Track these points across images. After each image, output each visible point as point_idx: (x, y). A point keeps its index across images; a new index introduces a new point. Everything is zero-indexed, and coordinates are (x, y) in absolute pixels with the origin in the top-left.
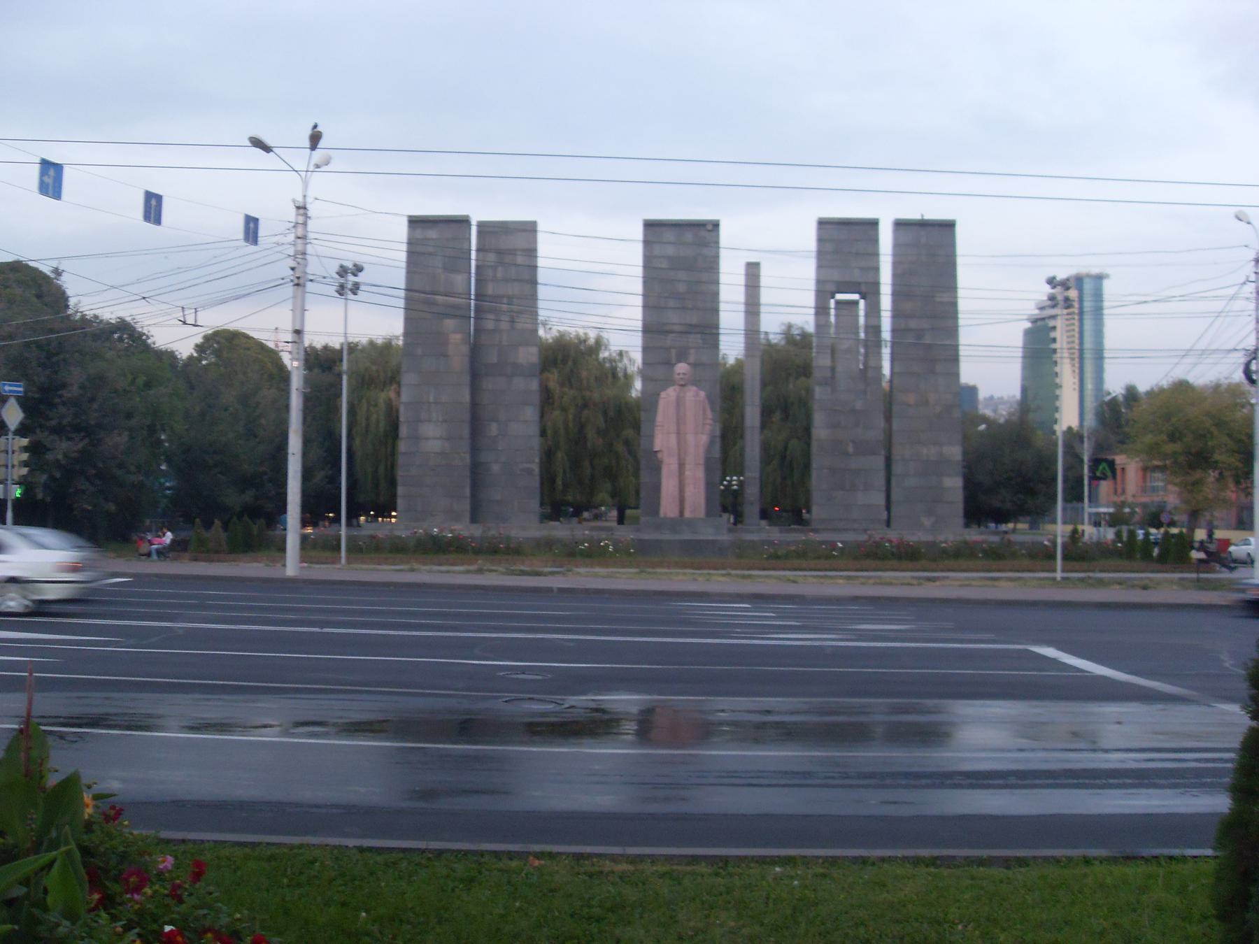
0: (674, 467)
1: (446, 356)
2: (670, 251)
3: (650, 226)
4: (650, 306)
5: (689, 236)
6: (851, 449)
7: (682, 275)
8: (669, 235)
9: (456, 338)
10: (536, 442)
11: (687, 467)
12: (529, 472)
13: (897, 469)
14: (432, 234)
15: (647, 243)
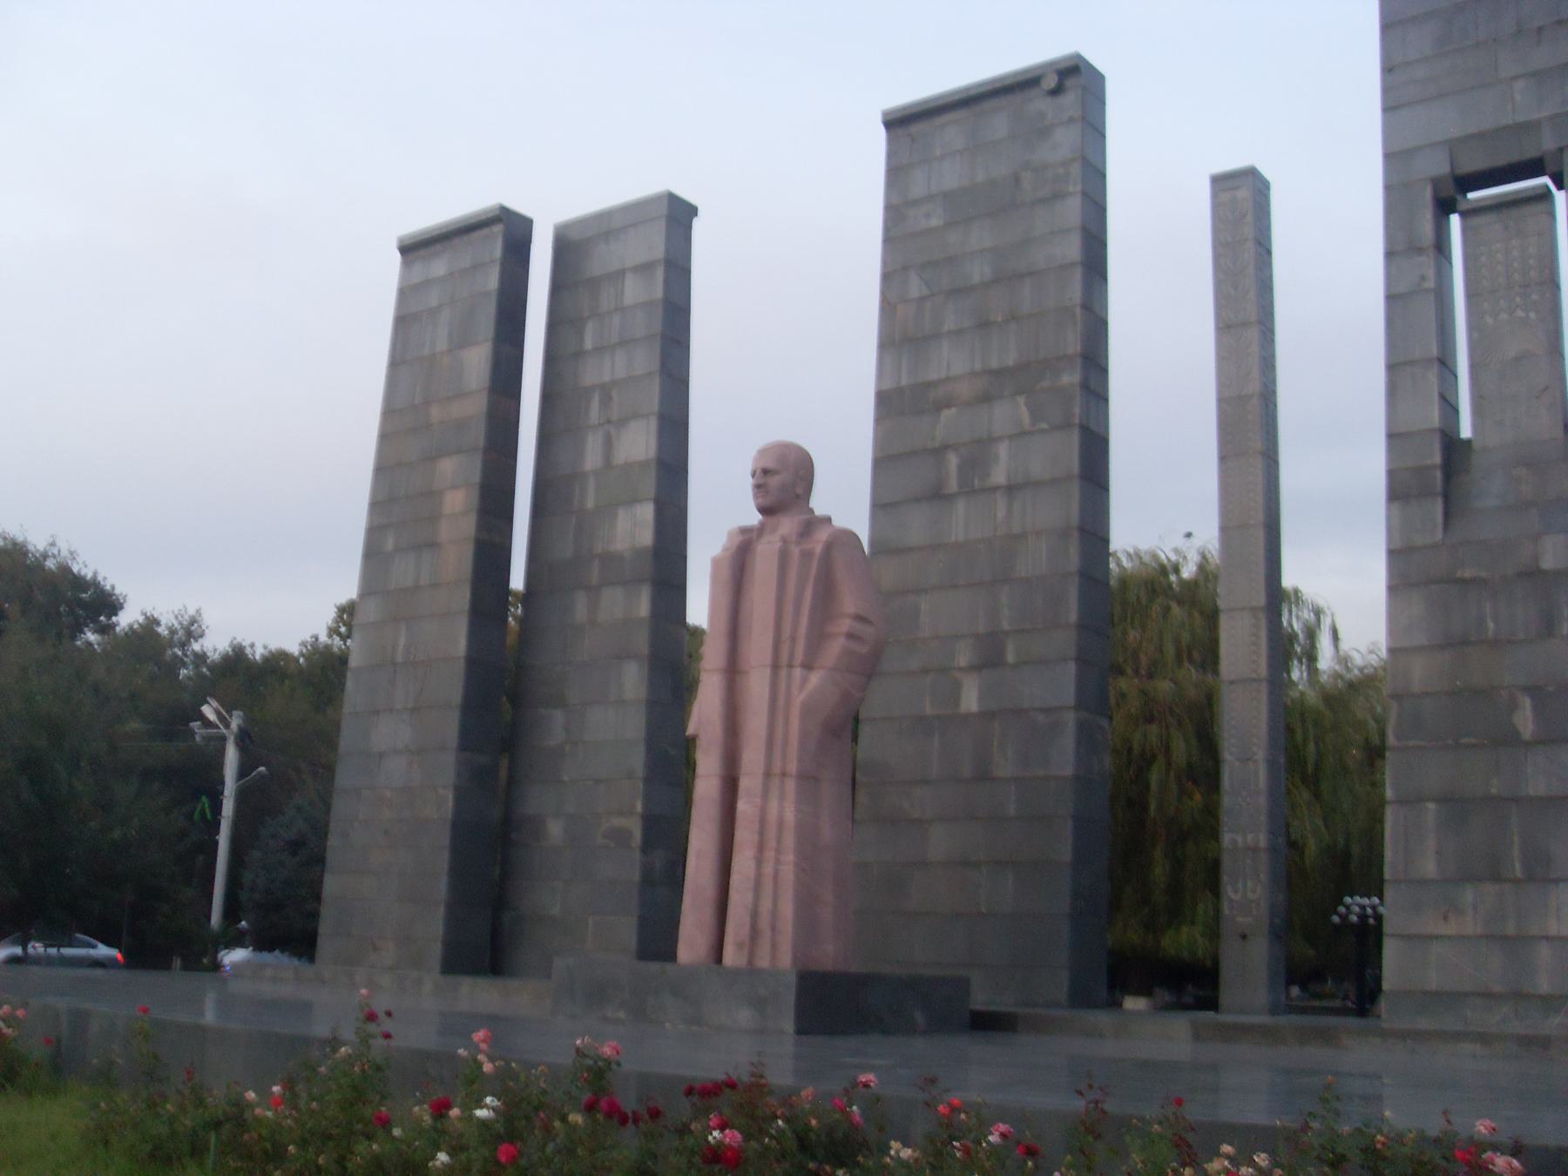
1: (433, 545)
2: (951, 176)
3: (899, 123)
4: (901, 335)
5: (998, 123)
6: (1525, 721)
7: (981, 236)
8: (951, 134)
10: (637, 760)
11: (745, 783)
12: (621, 836)
14: (439, 267)
15: (896, 173)
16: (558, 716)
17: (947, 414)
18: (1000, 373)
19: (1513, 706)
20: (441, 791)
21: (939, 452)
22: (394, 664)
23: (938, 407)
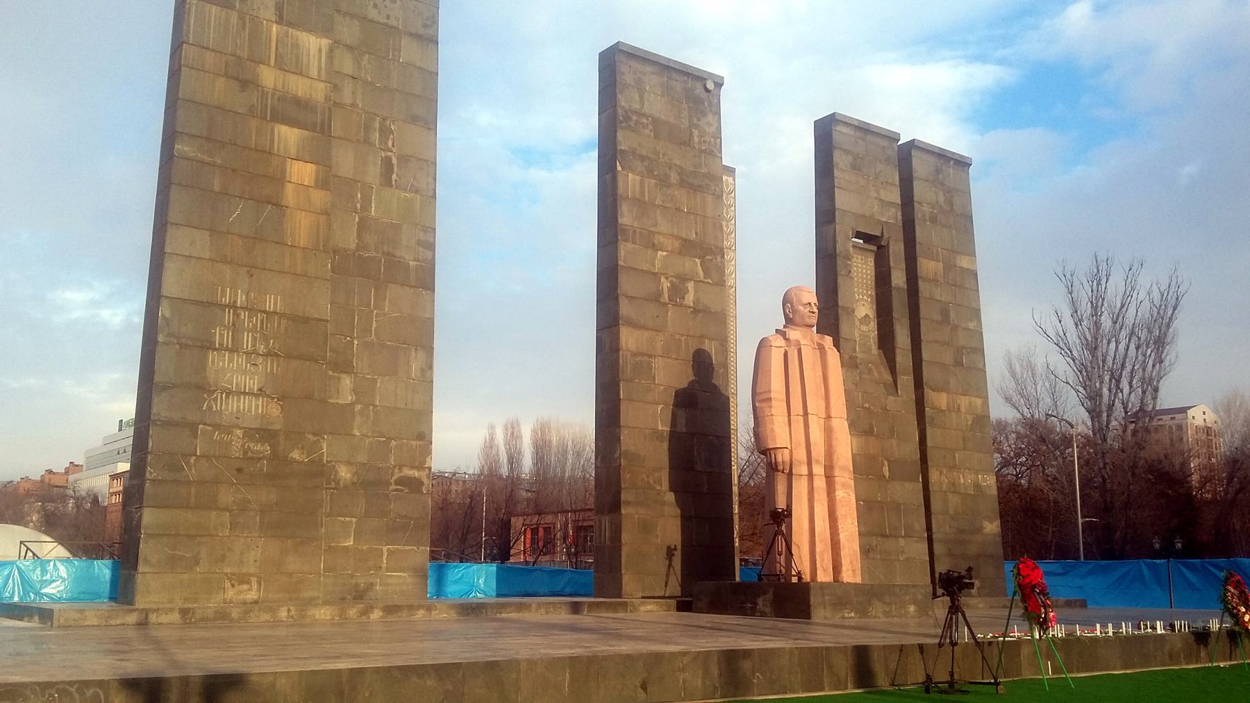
0: (820, 483)
1: (277, 205)
9: (302, 172)
13: (936, 506)
16: (347, 381)
17: (660, 253)
18: (685, 240)
19: (883, 465)
20: (310, 436)
21: (655, 276)
22: (233, 306)
23: (655, 247)
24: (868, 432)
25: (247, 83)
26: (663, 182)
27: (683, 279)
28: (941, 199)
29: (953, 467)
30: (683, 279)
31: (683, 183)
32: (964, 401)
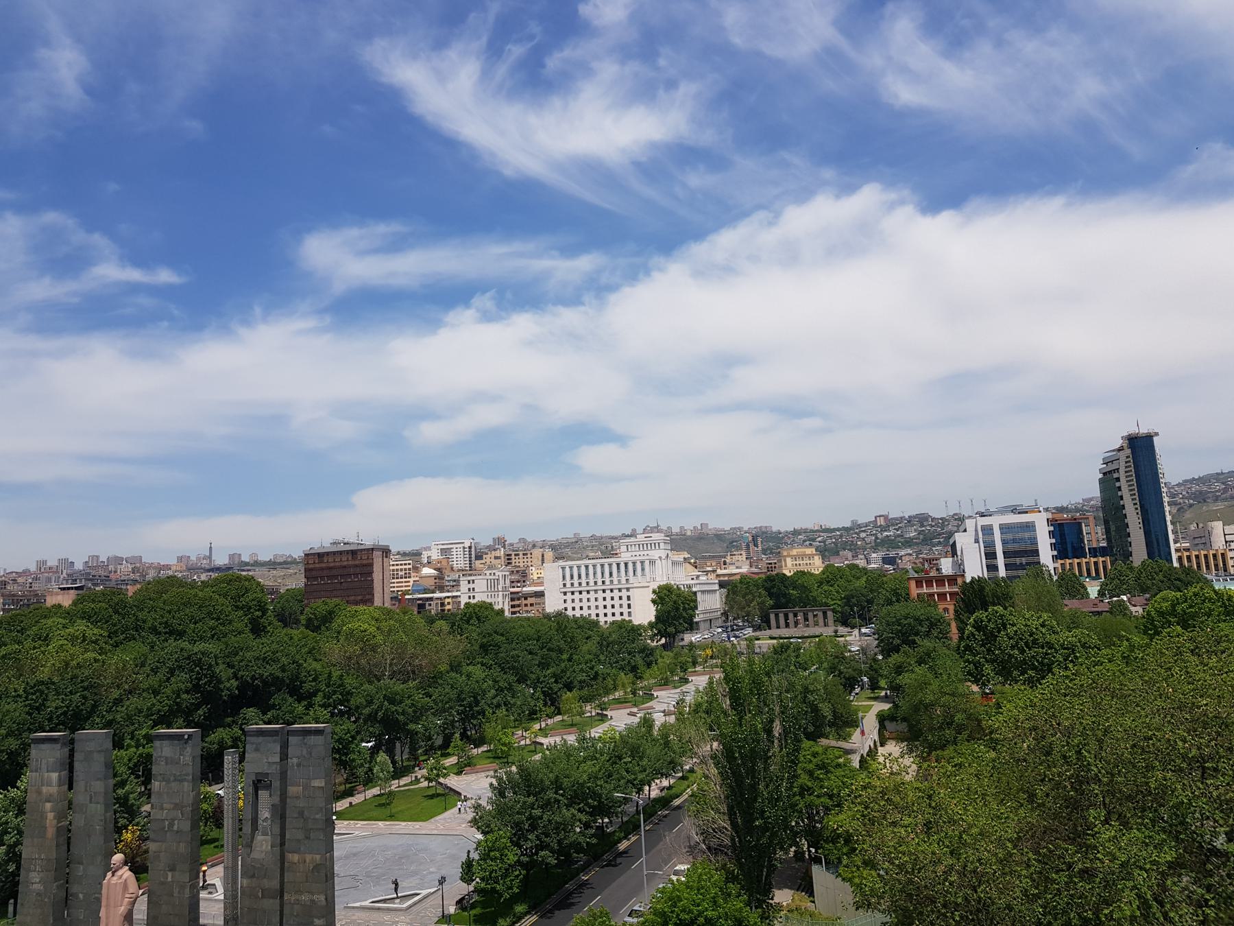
24: (253, 876)
25: (39, 792)
26: (168, 781)
27: (173, 820)
28: (305, 752)
29: (299, 892)
30: (173, 820)
31: (175, 780)
32: (308, 857)
